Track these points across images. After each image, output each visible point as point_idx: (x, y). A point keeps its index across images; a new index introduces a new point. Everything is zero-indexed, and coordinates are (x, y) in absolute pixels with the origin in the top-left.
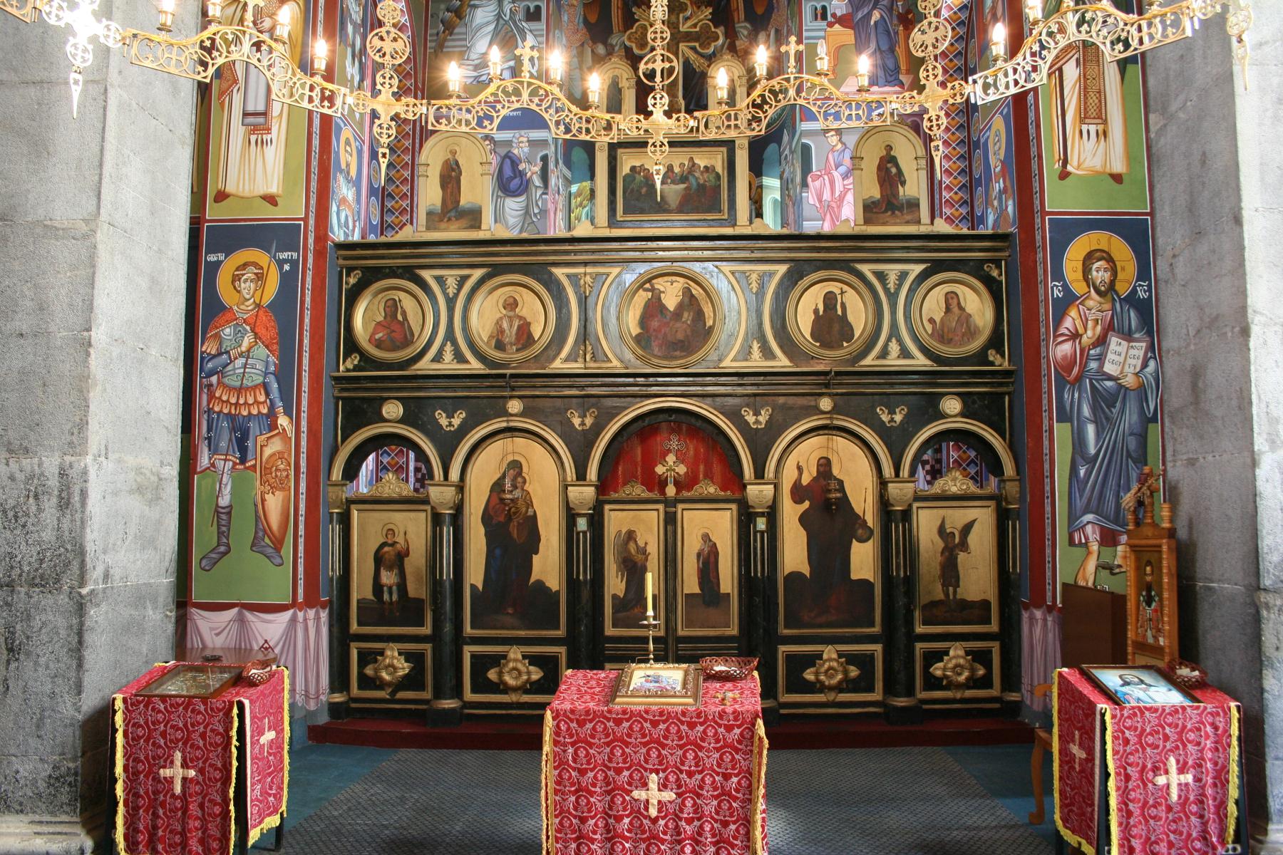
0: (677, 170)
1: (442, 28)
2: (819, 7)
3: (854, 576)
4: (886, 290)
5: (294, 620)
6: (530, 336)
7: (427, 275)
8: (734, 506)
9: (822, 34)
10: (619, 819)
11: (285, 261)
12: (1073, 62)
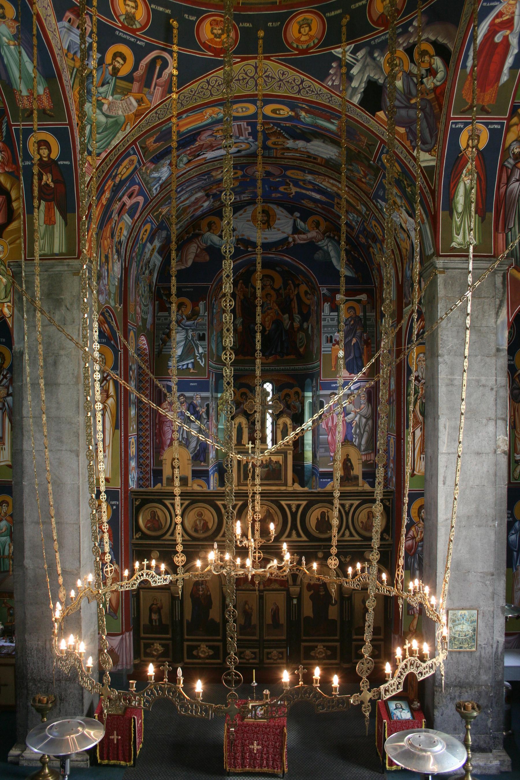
0: (264, 462)
3: (330, 618)
4: (345, 511)
5: (122, 639)
6: (208, 527)
8: (285, 592)
9: (330, 349)
10: (246, 753)
11: (114, 505)
12: (419, 429)
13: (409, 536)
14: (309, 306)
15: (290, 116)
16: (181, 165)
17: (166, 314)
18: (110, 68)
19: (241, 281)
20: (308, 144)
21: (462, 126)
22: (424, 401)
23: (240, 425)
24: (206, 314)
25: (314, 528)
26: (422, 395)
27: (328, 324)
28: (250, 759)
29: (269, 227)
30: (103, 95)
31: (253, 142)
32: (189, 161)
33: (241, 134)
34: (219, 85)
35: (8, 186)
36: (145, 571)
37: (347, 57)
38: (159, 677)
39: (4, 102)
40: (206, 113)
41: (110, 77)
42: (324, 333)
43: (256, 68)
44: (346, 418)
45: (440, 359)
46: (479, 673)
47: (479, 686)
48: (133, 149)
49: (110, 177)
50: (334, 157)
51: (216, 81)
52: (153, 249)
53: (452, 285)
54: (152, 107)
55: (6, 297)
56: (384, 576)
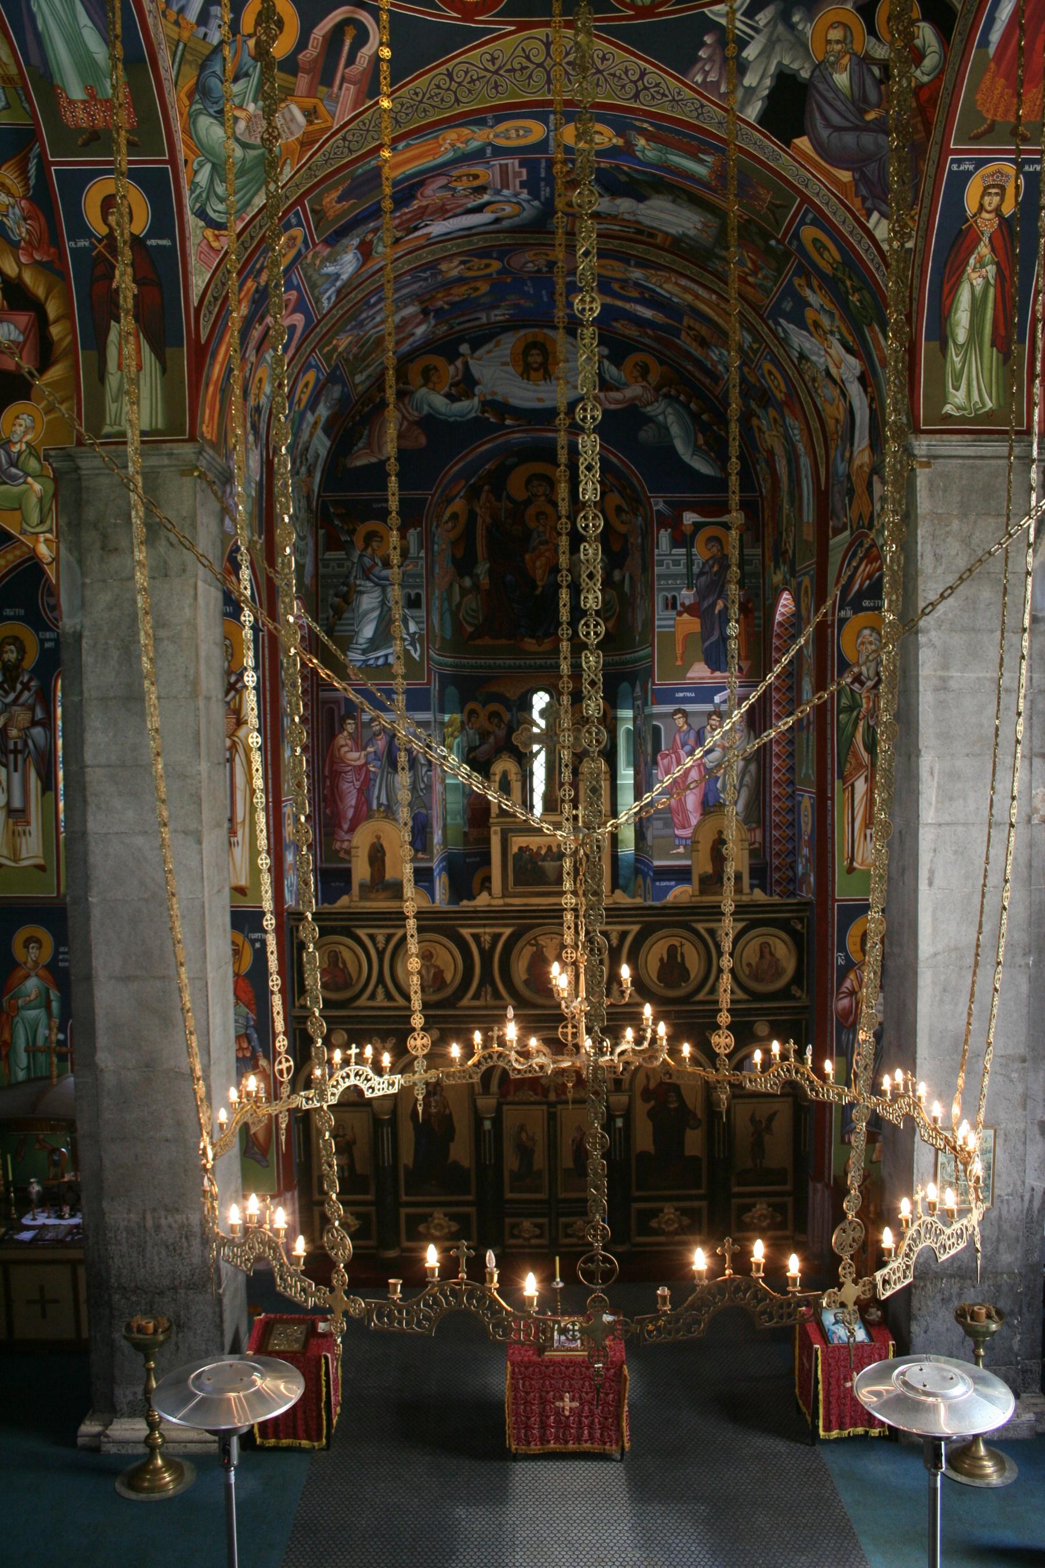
1: (331, 613)
2: (669, 596)
6: (443, 981)
7: (362, 933)
9: (671, 622)
10: (548, 1417)
11: (256, 940)
12: (862, 779)
13: (844, 989)
14: (625, 537)
15: (615, 147)
16: (380, 249)
17: (341, 554)
18: (252, 43)
19: (486, 488)
20: (641, 206)
21: (971, 167)
22: (872, 723)
23: (505, 775)
24: (422, 554)
25: (654, 977)
26: (868, 711)
27: (667, 572)
28: (557, 1428)
29: (547, 376)
30: (237, 101)
31: (528, 201)
32: (397, 241)
33: (505, 185)
34: (472, 81)
35: (40, 292)
36: (353, 1068)
37: (738, 24)
38: (449, 1268)
39: (34, 116)
40: (444, 140)
41: (252, 62)
42: (661, 590)
43: (548, 45)
44: (705, 760)
45: (922, 639)
46: (997, 1250)
47: (996, 1274)
48: (297, 214)
49: (250, 272)
50: (692, 233)
51: (466, 73)
52: (316, 423)
53: (945, 491)
54: (336, 127)
55: (42, 522)
56: (828, 1066)
